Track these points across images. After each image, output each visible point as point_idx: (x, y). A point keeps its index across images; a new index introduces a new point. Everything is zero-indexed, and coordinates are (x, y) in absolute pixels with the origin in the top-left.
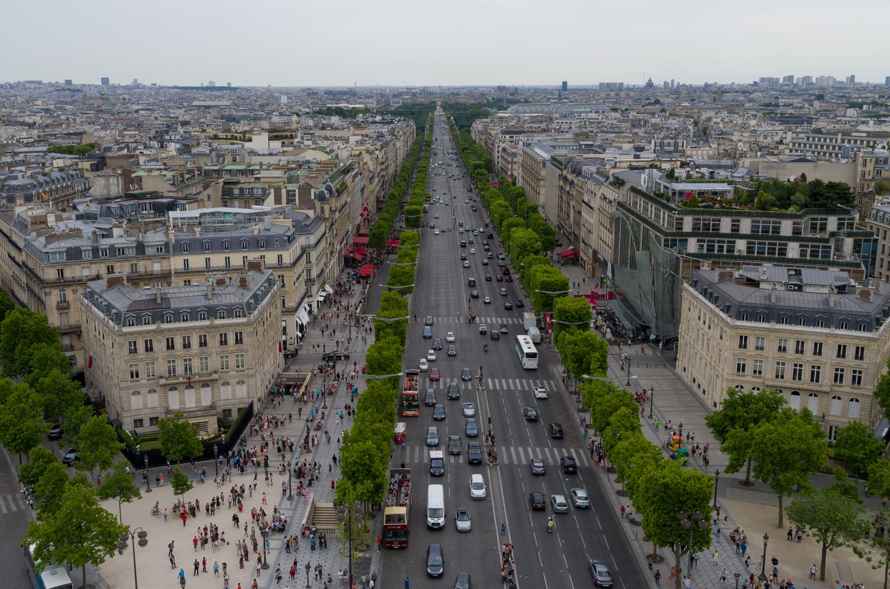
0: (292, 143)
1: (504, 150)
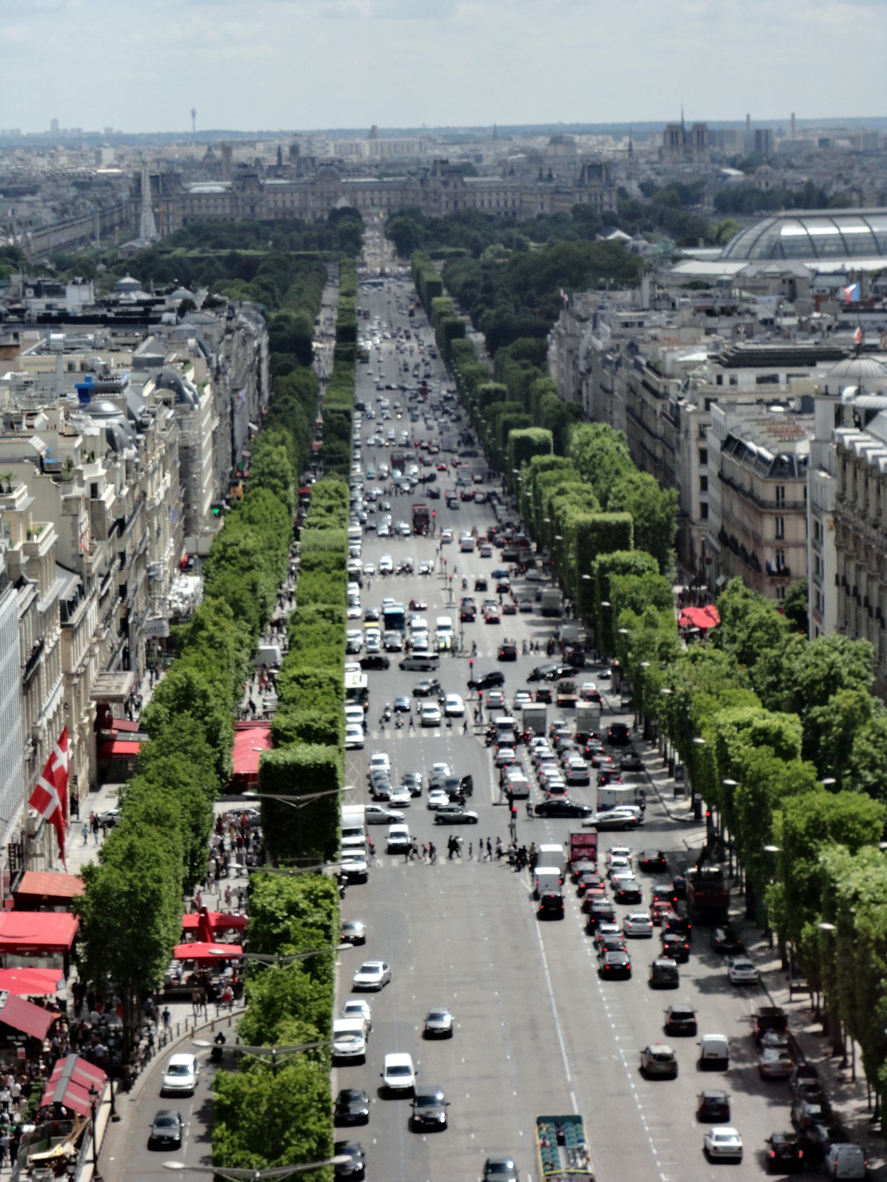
1: (733, 445)
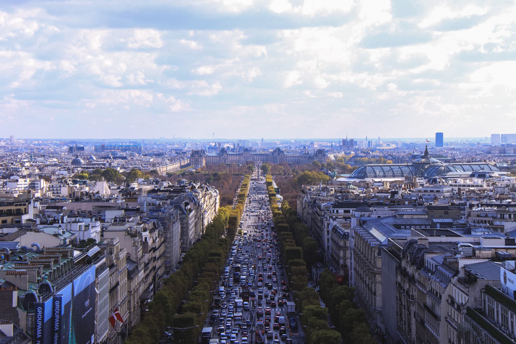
0: (19, 222)
1: (335, 229)
